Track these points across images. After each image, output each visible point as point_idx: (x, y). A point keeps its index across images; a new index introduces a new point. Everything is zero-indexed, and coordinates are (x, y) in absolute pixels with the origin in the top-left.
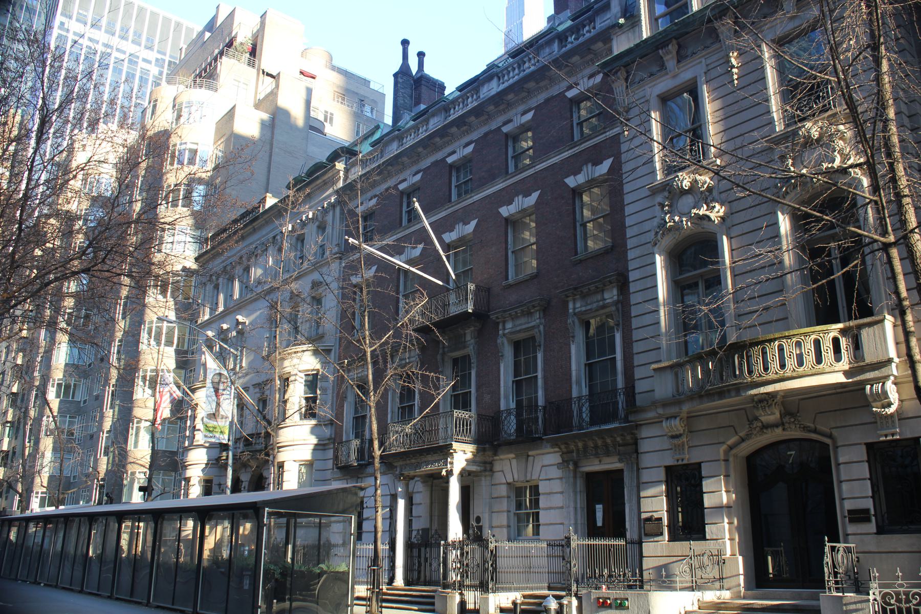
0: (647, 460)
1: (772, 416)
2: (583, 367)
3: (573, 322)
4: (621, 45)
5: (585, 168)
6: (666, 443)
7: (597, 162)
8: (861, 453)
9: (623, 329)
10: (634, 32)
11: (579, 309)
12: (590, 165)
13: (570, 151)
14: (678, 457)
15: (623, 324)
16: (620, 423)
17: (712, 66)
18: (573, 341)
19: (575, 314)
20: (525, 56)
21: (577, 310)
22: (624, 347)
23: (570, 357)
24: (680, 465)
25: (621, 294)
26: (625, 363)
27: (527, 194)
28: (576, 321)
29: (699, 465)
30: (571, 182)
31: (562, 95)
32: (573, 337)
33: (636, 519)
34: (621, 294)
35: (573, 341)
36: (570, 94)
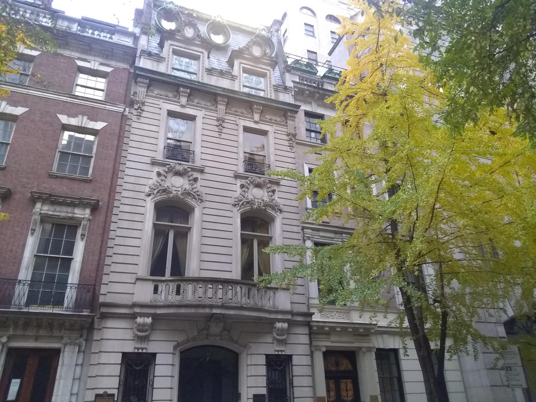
0: (108, 346)
1: (215, 329)
2: (33, 255)
3: (38, 218)
4: (144, 63)
5: (80, 117)
6: (129, 335)
7: (91, 119)
8: (262, 360)
9: (87, 240)
10: (158, 65)
11: (46, 212)
12: (85, 118)
13: (68, 99)
14: (139, 346)
15: (87, 237)
16: (67, 311)
17: (207, 117)
18: (32, 234)
19: (40, 214)
20: (43, 13)
21: (42, 212)
22: (84, 254)
23: (24, 246)
24: (140, 353)
25: (91, 215)
26: (82, 265)
27: (14, 103)
28: (39, 219)
29: (154, 355)
30: (64, 119)
31: (71, 60)
32: (34, 230)
33: (68, 394)
34: (91, 215)
35: (32, 234)
36: (80, 63)
